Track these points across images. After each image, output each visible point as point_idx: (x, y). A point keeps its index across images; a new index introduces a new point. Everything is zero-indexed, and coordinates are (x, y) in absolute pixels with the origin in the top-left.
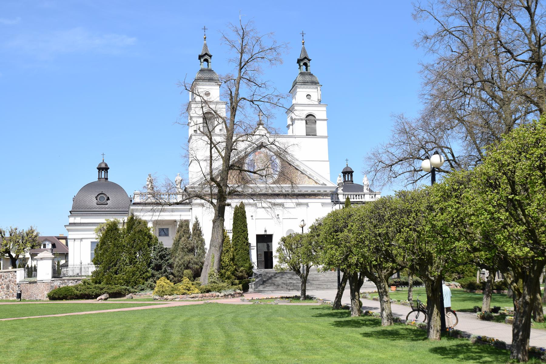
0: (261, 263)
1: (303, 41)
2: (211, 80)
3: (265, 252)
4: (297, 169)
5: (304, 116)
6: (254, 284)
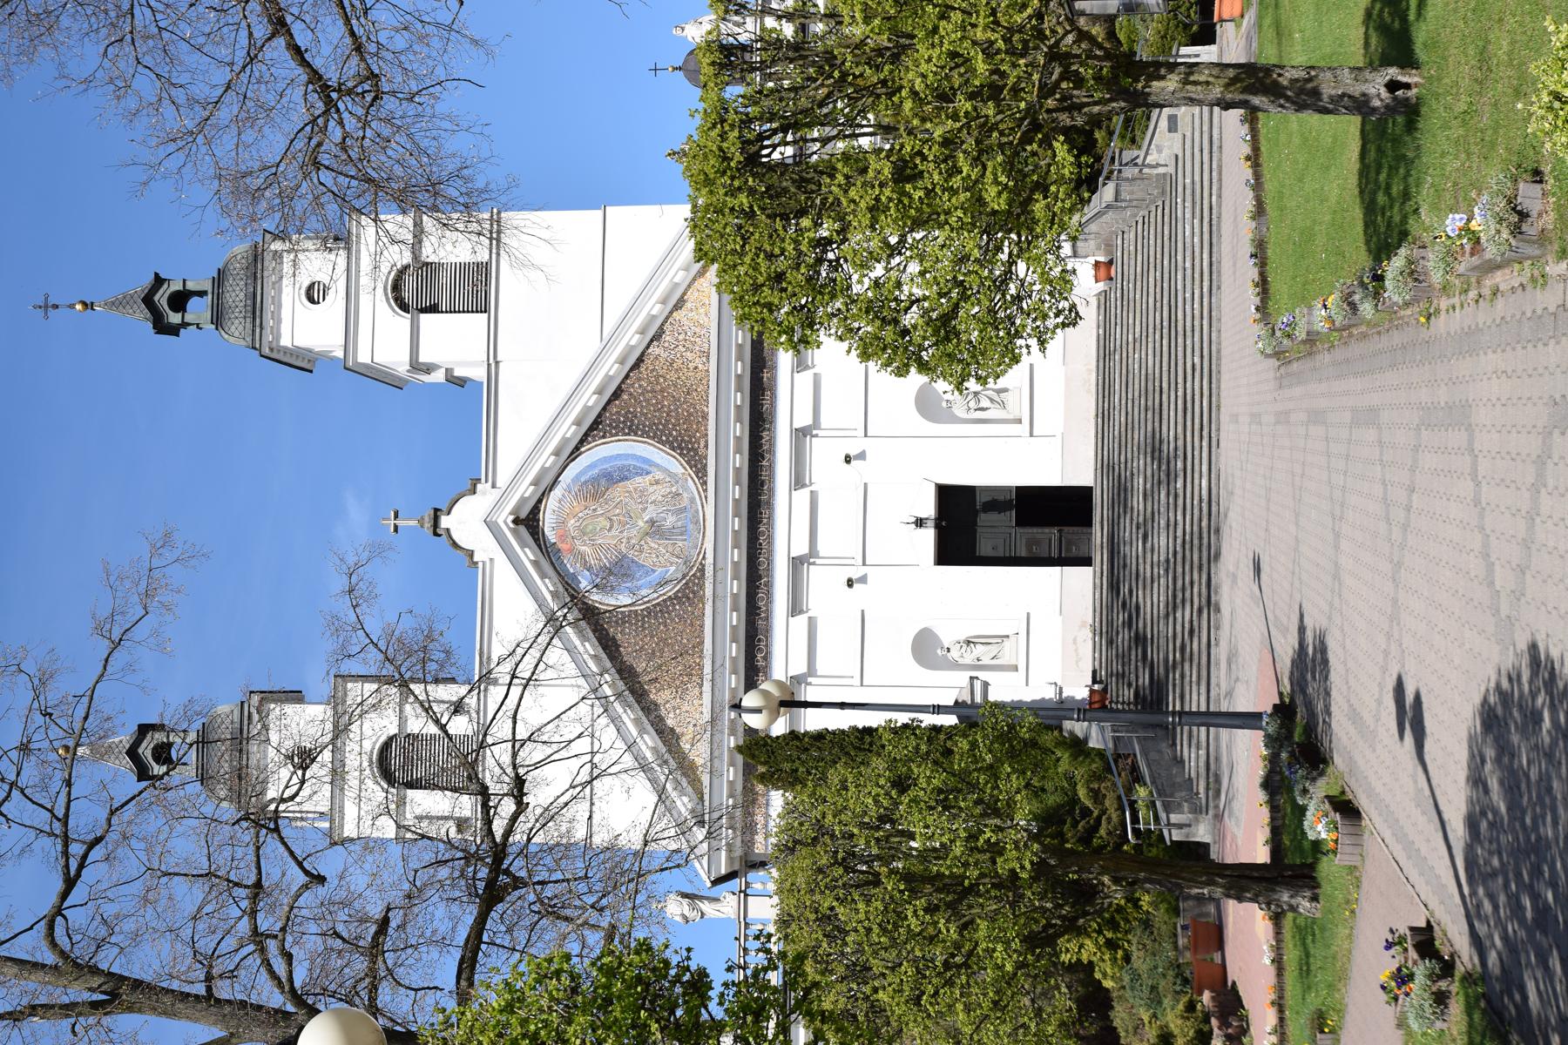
0: (1069, 543)
1: (79, 307)
2: (240, 740)
3: (1020, 522)
4: (640, 360)
5: (403, 321)
6: (1168, 812)
